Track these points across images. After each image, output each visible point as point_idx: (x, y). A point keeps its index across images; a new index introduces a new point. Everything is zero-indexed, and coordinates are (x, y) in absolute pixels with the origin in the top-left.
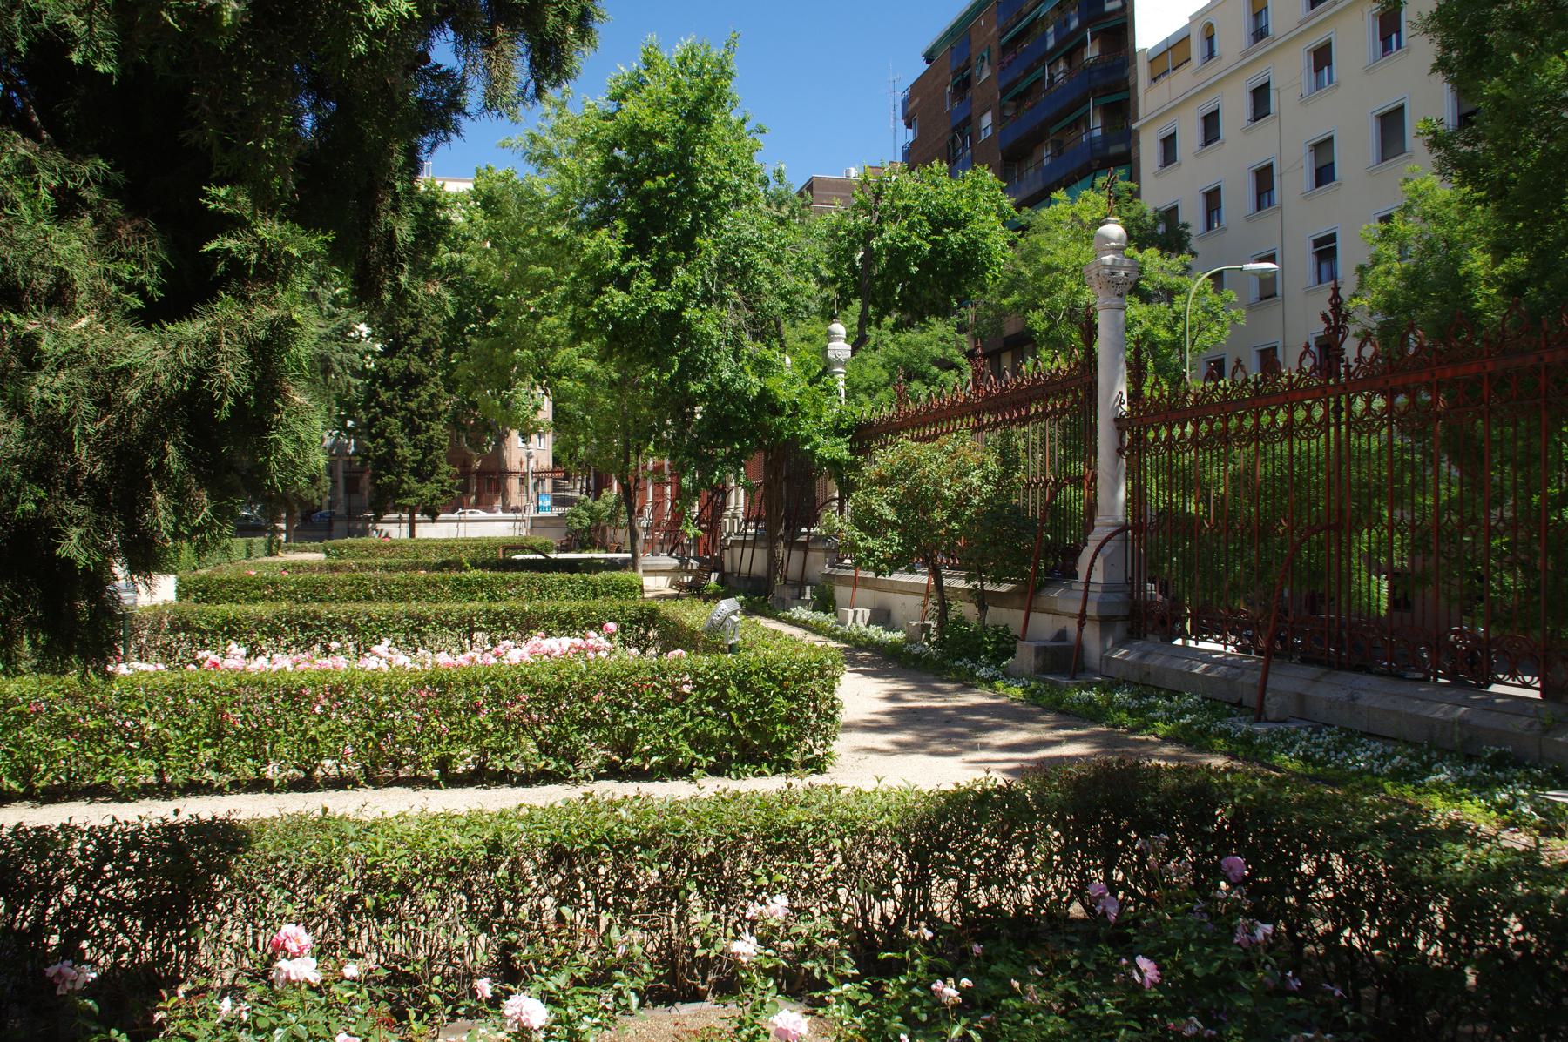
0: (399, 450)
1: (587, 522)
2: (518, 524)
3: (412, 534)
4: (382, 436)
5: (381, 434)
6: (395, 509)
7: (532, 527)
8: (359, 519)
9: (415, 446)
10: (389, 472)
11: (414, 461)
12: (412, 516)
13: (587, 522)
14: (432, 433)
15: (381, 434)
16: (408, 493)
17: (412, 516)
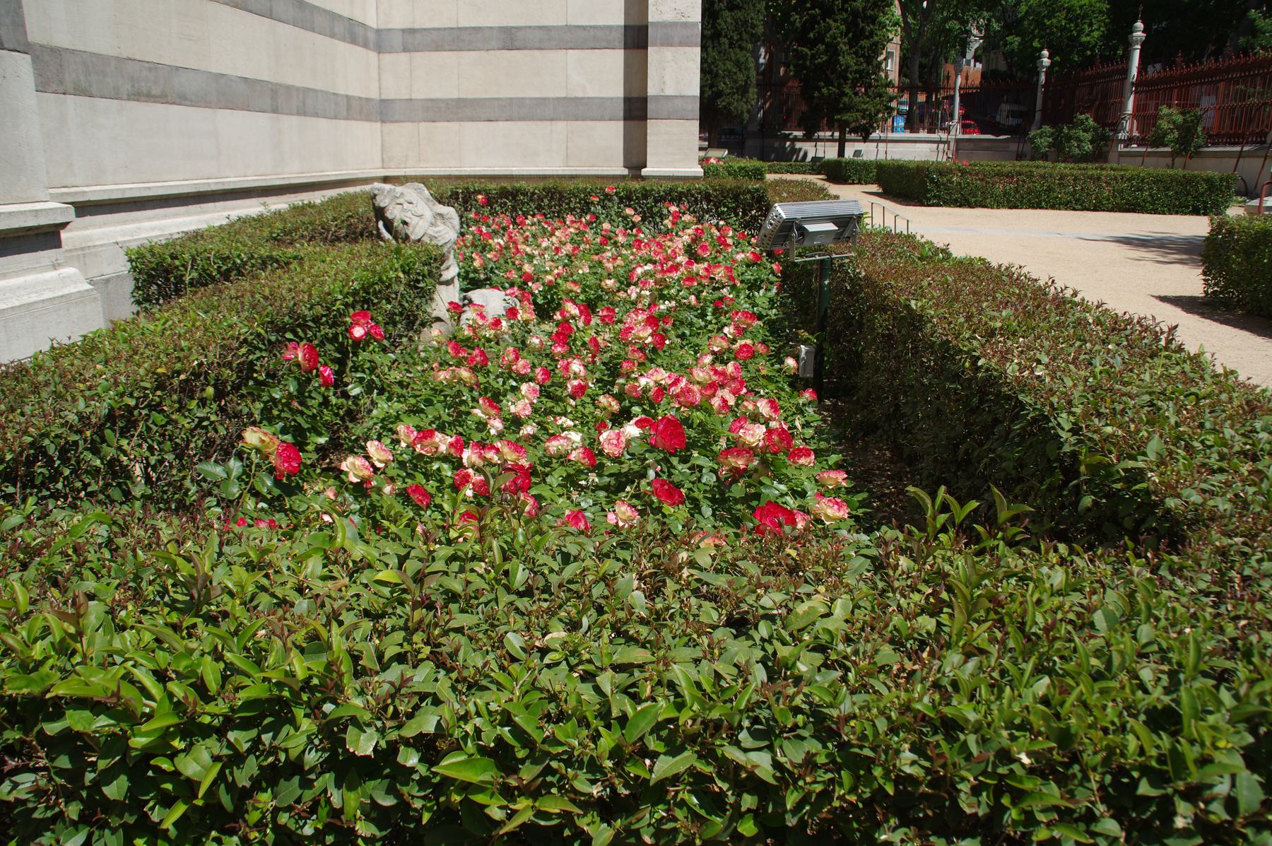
0: (841, 58)
1: (1088, 147)
2: (941, 146)
3: (841, 152)
4: (823, 42)
5: (820, 39)
6: (830, 127)
7: (957, 150)
8: (776, 137)
9: (855, 53)
10: (829, 83)
11: (856, 72)
12: (842, 134)
13: (1088, 147)
14: (876, 38)
15: (820, 39)
16: (848, 108)
17: (842, 134)
